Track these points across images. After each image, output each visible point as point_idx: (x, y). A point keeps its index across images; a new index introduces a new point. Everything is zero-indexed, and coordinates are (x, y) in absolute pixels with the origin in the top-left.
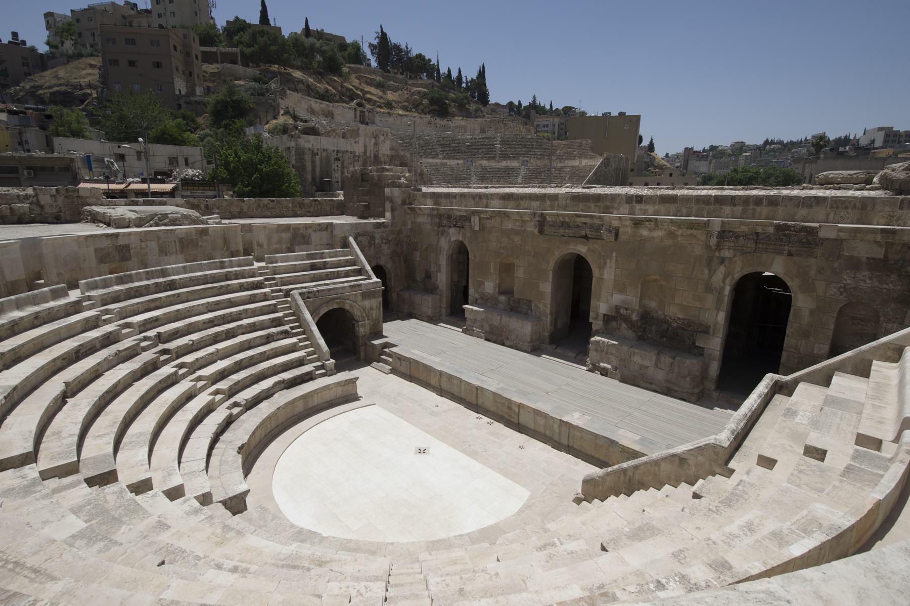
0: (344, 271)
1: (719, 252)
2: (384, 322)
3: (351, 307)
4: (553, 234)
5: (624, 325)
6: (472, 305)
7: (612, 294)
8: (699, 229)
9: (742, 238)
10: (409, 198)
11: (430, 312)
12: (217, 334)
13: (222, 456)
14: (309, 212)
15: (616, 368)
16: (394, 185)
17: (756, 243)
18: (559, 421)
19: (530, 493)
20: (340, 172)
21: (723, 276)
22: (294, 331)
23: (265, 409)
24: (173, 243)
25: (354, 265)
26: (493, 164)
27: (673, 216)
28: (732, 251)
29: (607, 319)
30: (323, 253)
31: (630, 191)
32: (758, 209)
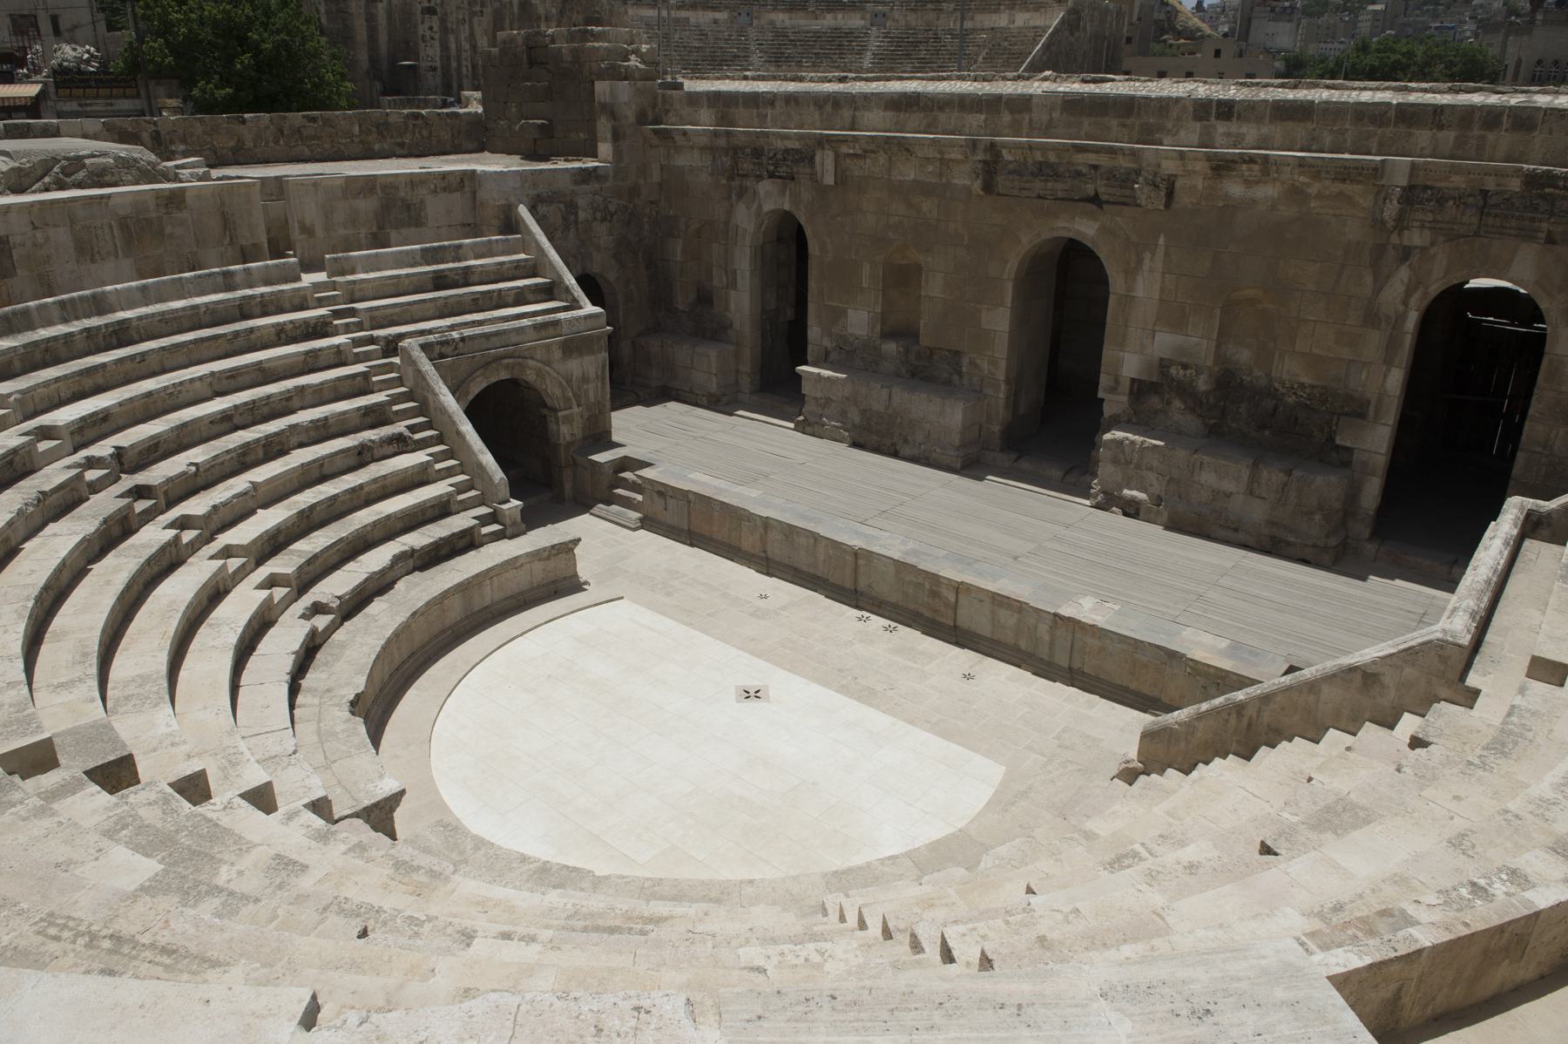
0: (512, 288)
1: (1399, 234)
2: (614, 409)
3: (538, 376)
4: (1015, 192)
5: (1177, 404)
6: (815, 365)
7: (1154, 332)
8: (1359, 182)
9: (1451, 203)
10: (654, 106)
11: (715, 386)
12: (246, 448)
13: (319, 722)
14: (402, 145)
15: (1158, 501)
16: (616, 74)
17: (1482, 214)
18: (1052, 617)
19: (1004, 768)
20: (437, 43)
21: (1404, 288)
22: (417, 436)
23: (384, 617)
24: (107, 230)
25: (534, 276)
26: (803, 22)
27: (1302, 150)
28: (1427, 232)
29: (1140, 389)
30: (460, 246)
31: (1196, 89)
32: (1491, 136)
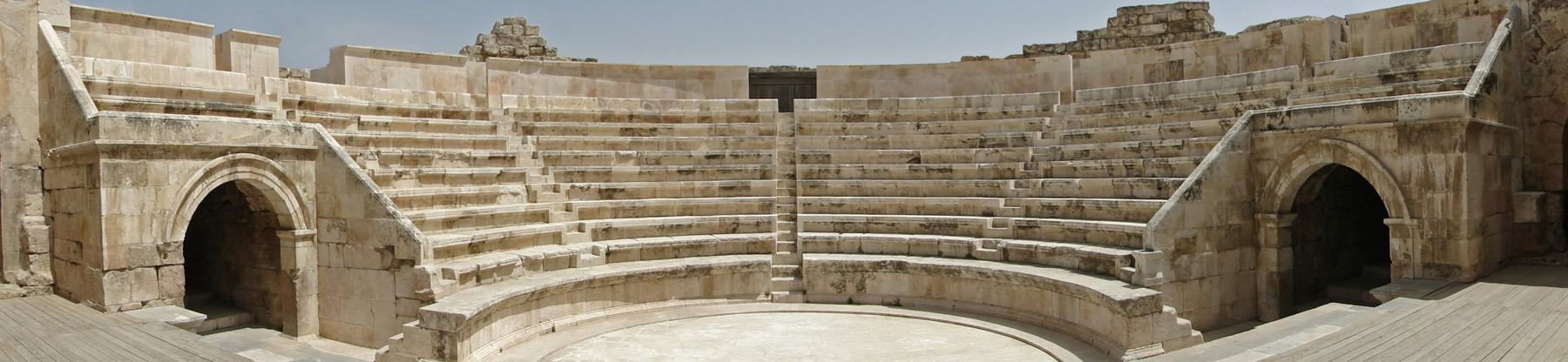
24: (1236, 57)
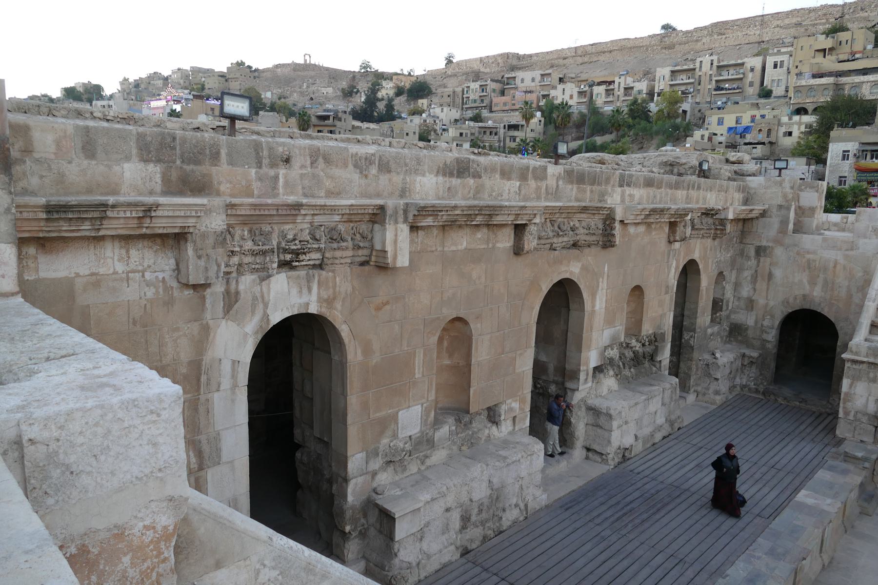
7: (603, 330)
